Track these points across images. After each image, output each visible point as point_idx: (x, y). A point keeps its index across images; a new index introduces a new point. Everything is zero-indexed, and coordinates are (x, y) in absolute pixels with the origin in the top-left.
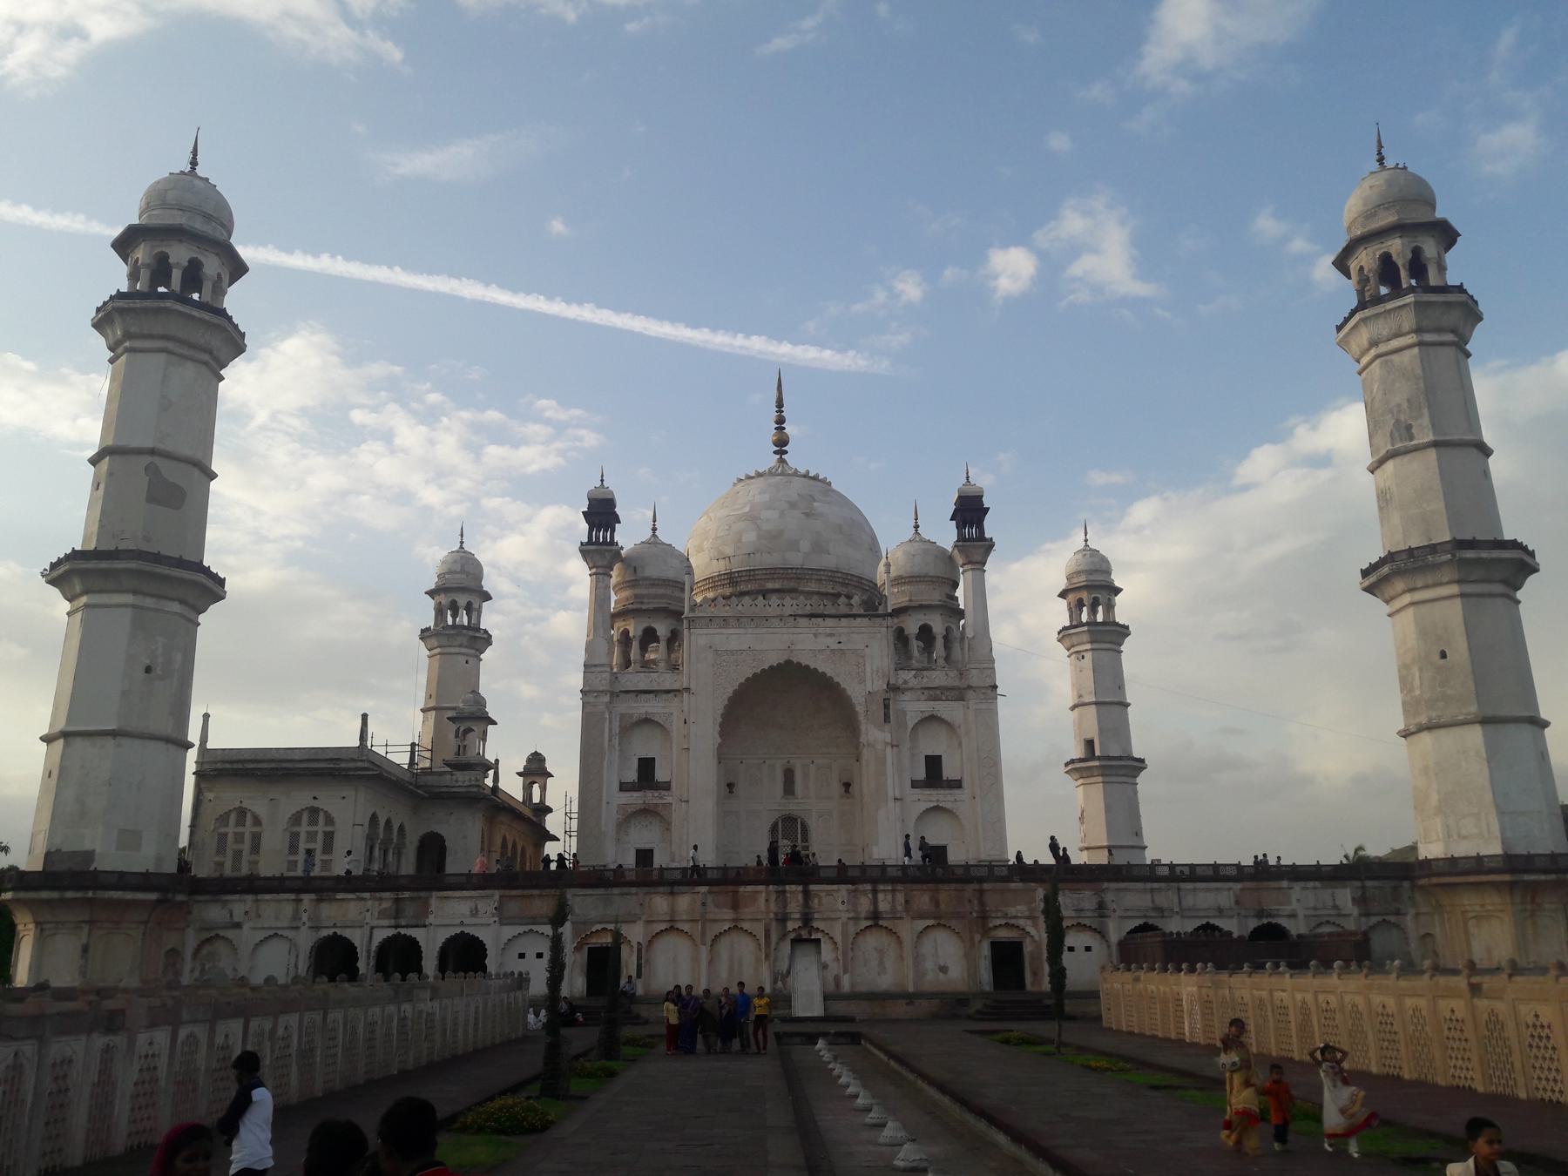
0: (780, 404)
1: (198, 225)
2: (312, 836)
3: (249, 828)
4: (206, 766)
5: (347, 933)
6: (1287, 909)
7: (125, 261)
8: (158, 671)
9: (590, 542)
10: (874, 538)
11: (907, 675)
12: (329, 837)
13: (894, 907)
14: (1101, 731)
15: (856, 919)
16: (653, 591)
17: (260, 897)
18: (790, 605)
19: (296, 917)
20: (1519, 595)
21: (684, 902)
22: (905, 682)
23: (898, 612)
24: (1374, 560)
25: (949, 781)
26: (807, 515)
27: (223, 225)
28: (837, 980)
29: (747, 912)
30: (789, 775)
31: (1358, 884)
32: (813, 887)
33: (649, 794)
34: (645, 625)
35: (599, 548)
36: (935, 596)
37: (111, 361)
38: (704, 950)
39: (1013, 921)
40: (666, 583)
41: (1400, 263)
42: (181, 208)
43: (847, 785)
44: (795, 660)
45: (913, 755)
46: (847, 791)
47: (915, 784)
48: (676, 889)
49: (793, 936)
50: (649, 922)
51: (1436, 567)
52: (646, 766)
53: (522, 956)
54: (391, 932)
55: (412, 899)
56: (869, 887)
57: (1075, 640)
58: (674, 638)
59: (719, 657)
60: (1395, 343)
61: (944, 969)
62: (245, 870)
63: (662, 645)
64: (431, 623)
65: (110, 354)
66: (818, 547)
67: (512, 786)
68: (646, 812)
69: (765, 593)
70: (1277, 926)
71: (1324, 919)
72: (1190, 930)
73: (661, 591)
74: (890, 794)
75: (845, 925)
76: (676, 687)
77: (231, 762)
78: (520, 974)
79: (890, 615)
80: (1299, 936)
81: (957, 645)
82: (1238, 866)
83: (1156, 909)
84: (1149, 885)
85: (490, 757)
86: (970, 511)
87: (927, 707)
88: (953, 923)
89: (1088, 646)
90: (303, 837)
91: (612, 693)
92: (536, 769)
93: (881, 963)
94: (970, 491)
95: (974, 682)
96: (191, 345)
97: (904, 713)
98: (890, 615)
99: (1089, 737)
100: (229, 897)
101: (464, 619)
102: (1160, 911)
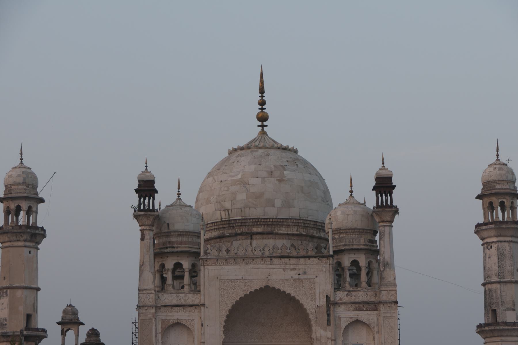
0: (262, 91)
9: (140, 210)
10: (326, 192)
11: (341, 295)
16: (180, 239)
22: (341, 299)
26: (280, 181)
35: (147, 215)
40: (188, 233)
57: (485, 234)
58: (194, 272)
66: (288, 204)
69: (251, 235)
73: (185, 239)
76: (196, 302)
79: (332, 256)
86: (384, 185)
87: (354, 315)
89: (495, 239)
94: (384, 173)
97: (340, 318)
98: (332, 256)
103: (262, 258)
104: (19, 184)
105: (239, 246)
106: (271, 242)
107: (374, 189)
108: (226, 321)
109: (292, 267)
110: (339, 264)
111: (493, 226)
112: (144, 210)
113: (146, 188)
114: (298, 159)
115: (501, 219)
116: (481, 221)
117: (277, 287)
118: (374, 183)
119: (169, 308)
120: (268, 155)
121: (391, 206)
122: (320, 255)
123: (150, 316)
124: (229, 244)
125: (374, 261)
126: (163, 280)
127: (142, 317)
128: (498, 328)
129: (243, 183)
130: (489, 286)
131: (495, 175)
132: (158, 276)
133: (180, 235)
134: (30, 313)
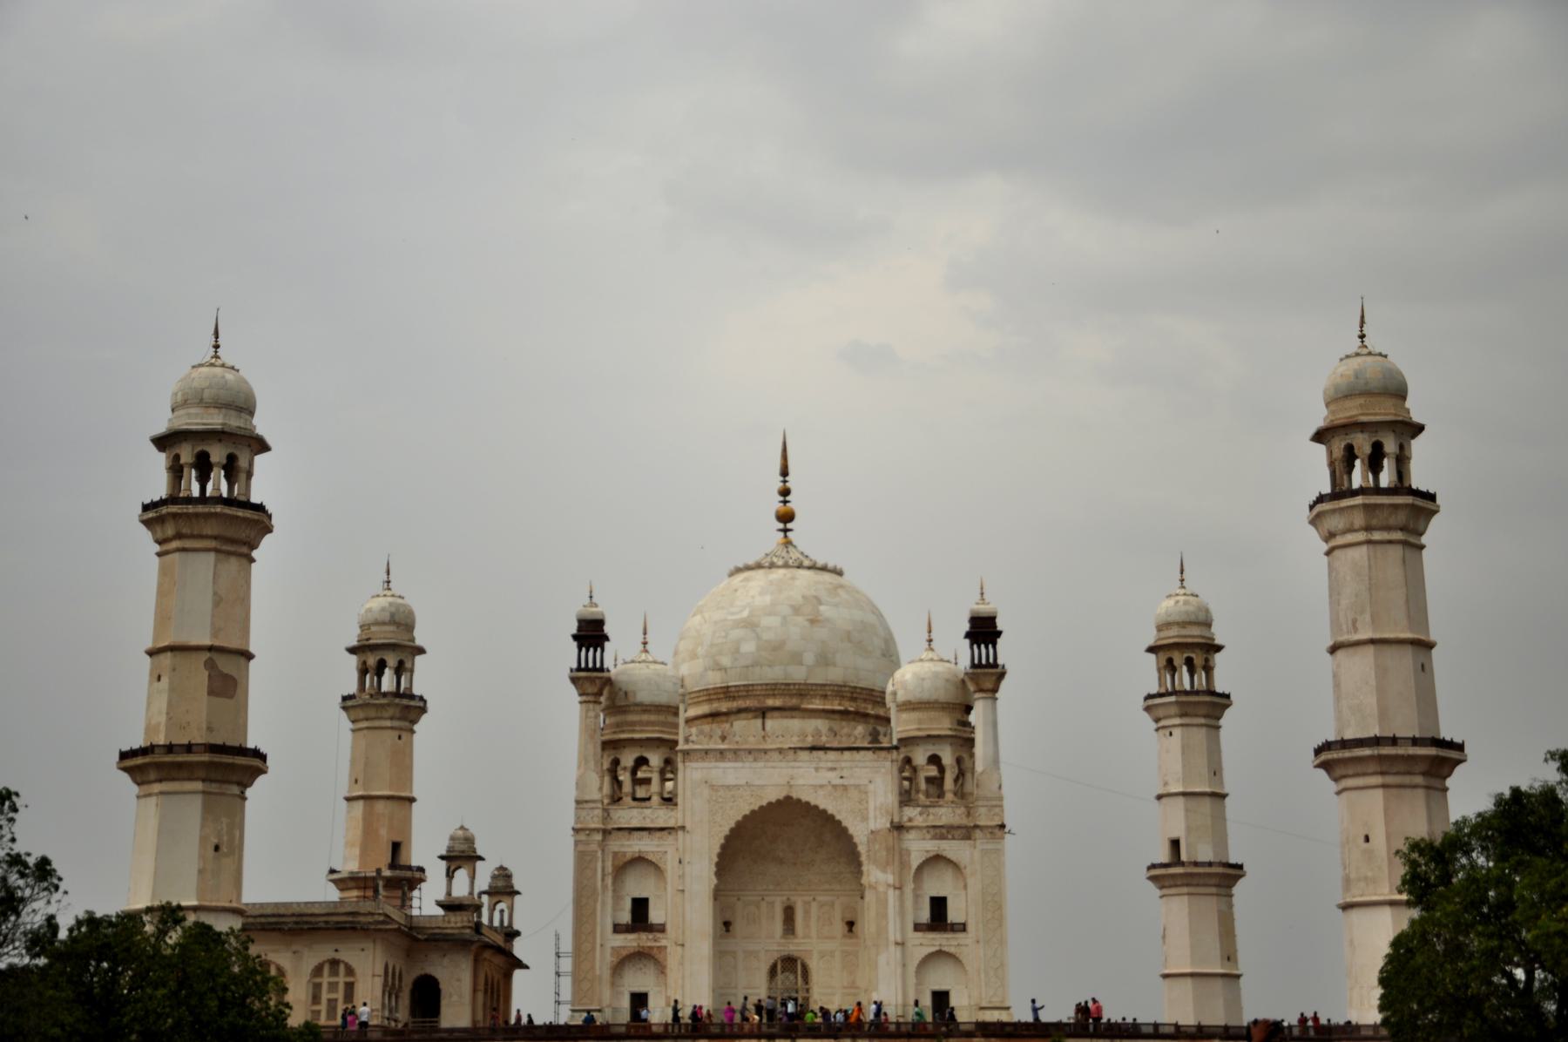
0: (785, 473)
2: (333, 987)
8: (224, 849)
9: (579, 669)
11: (910, 812)
12: (350, 987)
14: (1189, 829)
16: (645, 717)
22: (910, 820)
23: (906, 741)
25: (953, 924)
26: (813, 622)
30: (789, 913)
33: (644, 936)
34: (636, 755)
37: (159, 554)
43: (851, 924)
44: (794, 795)
45: (917, 897)
46: (850, 930)
47: (918, 927)
52: (640, 906)
57: (1160, 712)
59: (716, 790)
60: (1350, 538)
64: (352, 688)
65: (157, 548)
66: (824, 660)
68: (641, 956)
69: (763, 713)
73: (653, 718)
74: (892, 938)
76: (671, 824)
79: (896, 748)
82: (1177, 1026)
86: (983, 630)
94: (984, 610)
95: (981, 823)
96: (233, 541)
97: (909, 852)
98: (896, 748)
99: (1174, 835)
104: (384, 623)
105: (745, 730)
106: (795, 724)
107: (968, 635)
108: (720, 856)
109: (830, 765)
110: (908, 761)
111: (1173, 699)
112: (587, 669)
113: (591, 634)
114: (841, 586)
115: (1188, 687)
116: (1154, 690)
117: (804, 798)
118: (966, 627)
120: (793, 578)
121: (995, 665)
122: (875, 745)
123: (594, 847)
124: (727, 726)
125: (965, 756)
127: (581, 848)
129: (750, 624)
132: (607, 779)
134: (397, 839)
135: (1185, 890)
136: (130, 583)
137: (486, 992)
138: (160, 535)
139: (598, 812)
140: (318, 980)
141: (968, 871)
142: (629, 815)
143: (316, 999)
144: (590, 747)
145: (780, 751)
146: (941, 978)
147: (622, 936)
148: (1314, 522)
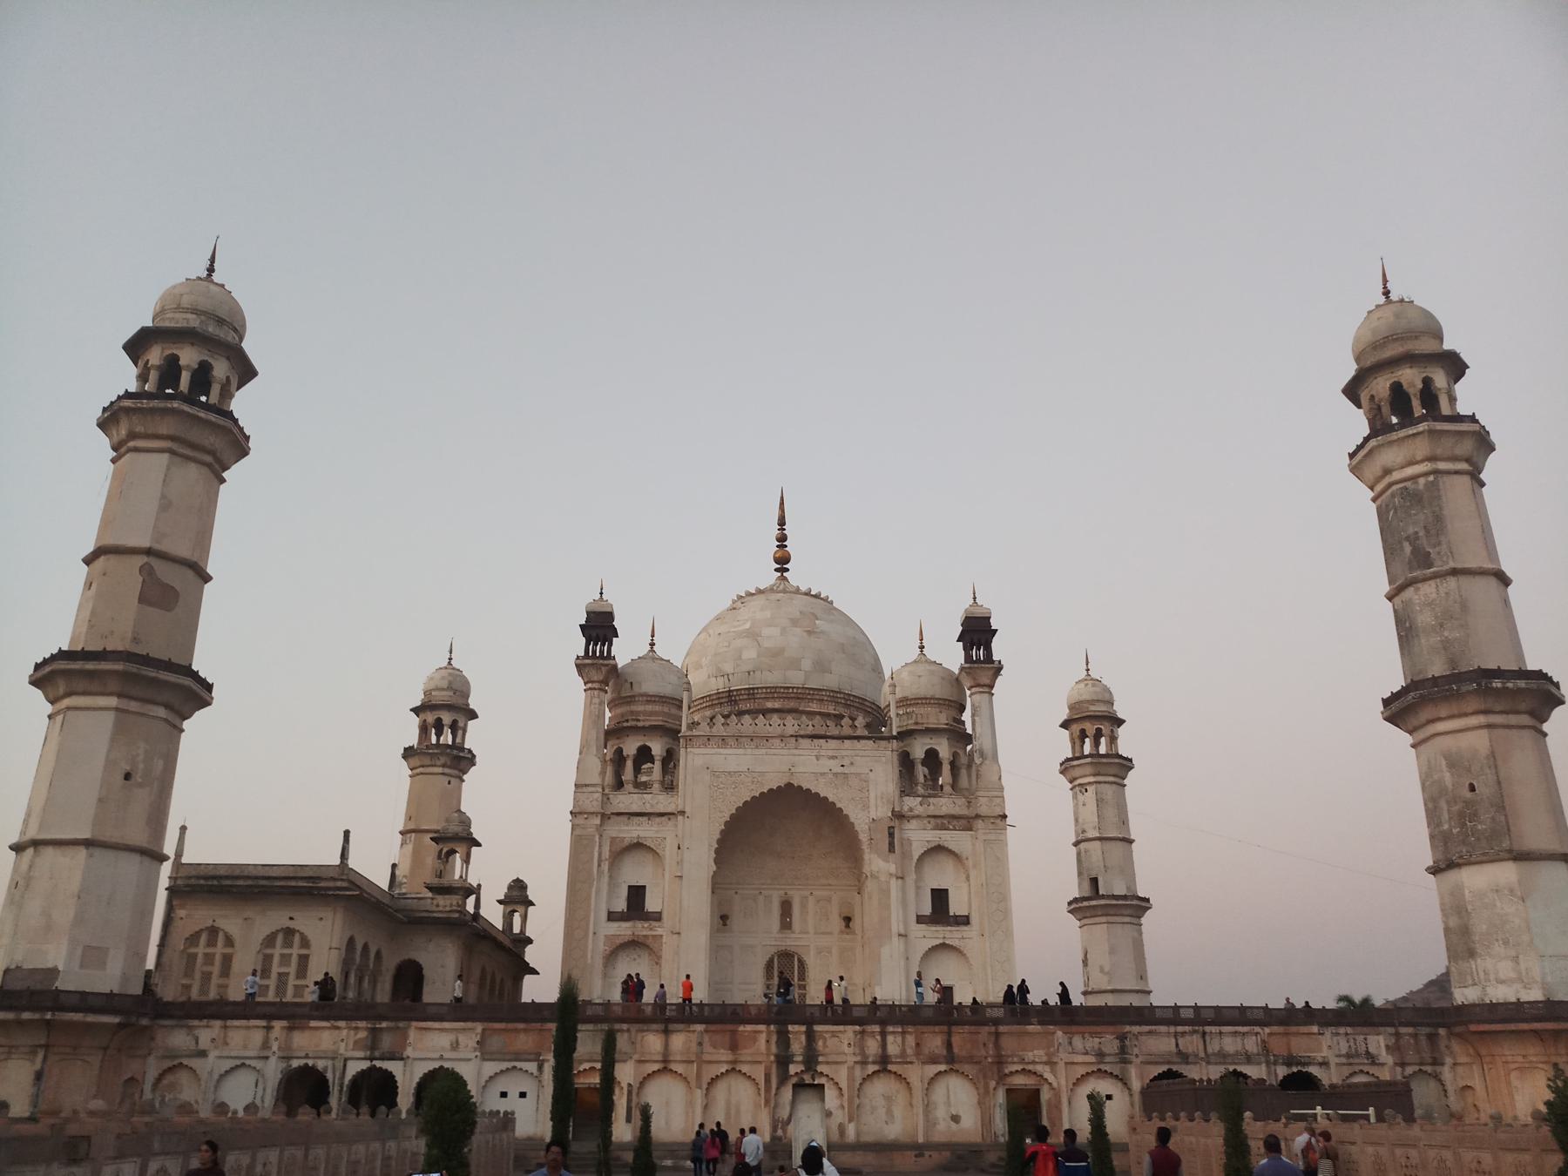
0: (782, 522)
1: (212, 329)
2: (285, 959)
3: (220, 949)
4: (179, 882)
5: (320, 1064)
6: (1319, 1056)
7: (136, 364)
11: (911, 803)
13: (903, 1051)
15: (864, 1063)
16: (649, 708)
17: (229, 1023)
18: (791, 724)
19: (266, 1045)
20: (1546, 727)
21: (678, 1041)
22: (911, 810)
23: (904, 735)
24: (1396, 689)
25: (956, 916)
26: (809, 633)
27: (235, 330)
28: (842, 1129)
29: (746, 1054)
30: (786, 908)
31: (1391, 1030)
32: (817, 1028)
33: (639, 924)
36: (941, 719)
37: (114, 461)
38: (699, 1094)
39: (1030, 1067)
41: (1411, 391)
42: (195, 311)
43: (848, 920)
45: (918, 888)
46: (847, 926)
47: (920, 919)
48: (671, 1027)
49: (794, 1080)
50: (640, 1062)
51: (1459, 696)
53: (504, 1095)
54: (365, 1065)
55: (388, 1029)
56: (877, 1028)
57: (1077, 772)
61: (956, 1119)
62: (213, 995)
63: (657, 766)
64: (413, 740)
66: (821, 666)
67: (493, 914)
68: (634, 944)
69: (765, 712)
70: (1309, 1075)
71: (1357, 1068)
72: (1218, 1076)
73: (657, 708)
75: (851, 1069)
77: (206, 878)
78: (506, 1113)
80: (1332, 1086)
81: (964, 772)
83: (1180, 1053)
84: (1172, 1029)
85: (473, 880)
86: (977, 632)
88: (967, 1068)
89: (1092, 779)
90: (276, 960)
91: (603, 815)
92: (517, 896)
93: (889, 1112)
94: (978, 612)
95: (984, 810)
100: (196, 1023)
101: (447, 738)
102: (1184, 1057)
103: (782, 737)
109: (830, 753)
113: (599, 627)
117: (805, 786)
119: (625, 818)
123: (591, 830)
126: (618, 774)
127: (578, 832)
128: (1102, 902)
129: (753, 635)
130: (1082, 846)
131: (1086, 693)
133: (648, 702)
135: (1104, 919)
136: (73, 486)
137: (481, 986)
138: (116, 439)
139: (598, 796)
140: (268, 951)
141: (970, 863)
142: (628, 801)
143: (266, 973)
144: (593, 734)
145: (782, 737)
146: (946, 971)
147: (615, 925)
148: (1355, 470)
